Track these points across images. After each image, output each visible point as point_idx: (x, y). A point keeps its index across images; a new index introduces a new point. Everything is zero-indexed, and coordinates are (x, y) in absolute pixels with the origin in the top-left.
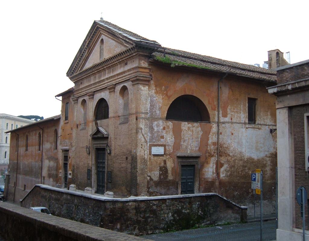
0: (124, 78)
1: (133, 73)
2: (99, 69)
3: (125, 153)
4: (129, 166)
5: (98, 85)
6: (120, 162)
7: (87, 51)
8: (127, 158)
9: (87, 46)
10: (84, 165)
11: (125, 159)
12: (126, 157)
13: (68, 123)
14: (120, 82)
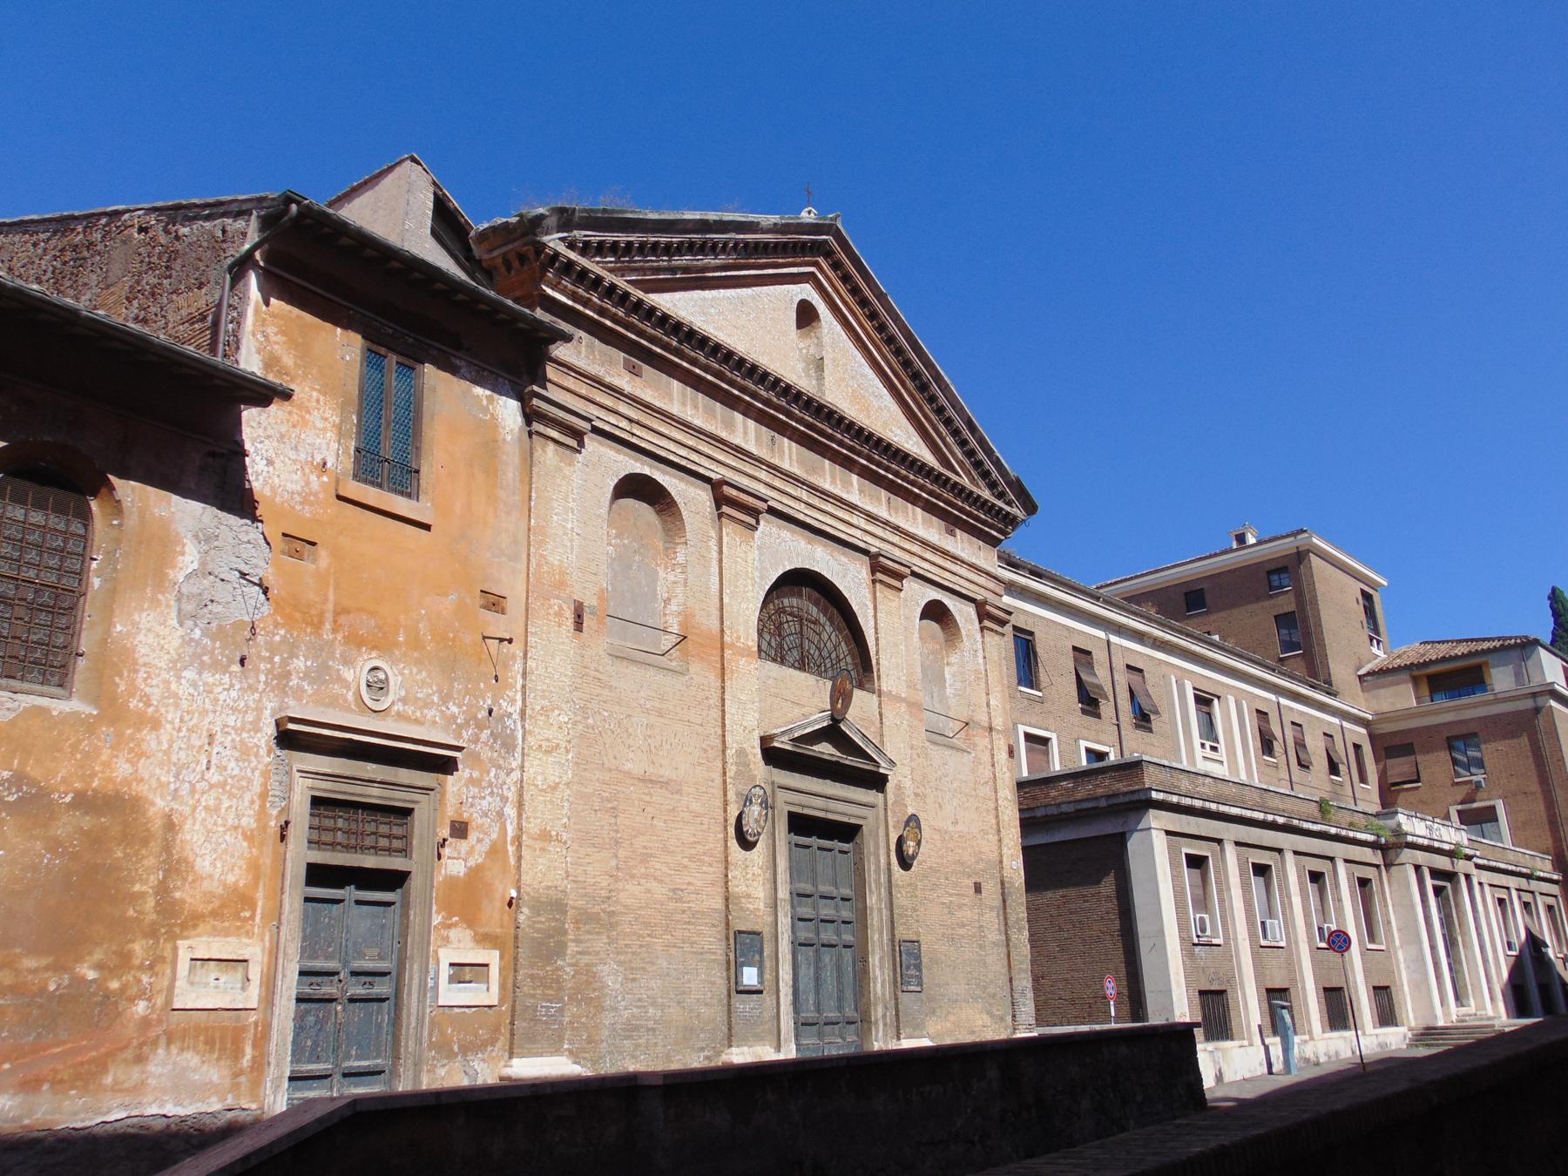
0: (947, 575)
2: (830, 438)
3: (968, 867)
6: (951, 902)
8: (978, 888)
10: (680, 900)
12: (975, 883)
13: (427, 527)
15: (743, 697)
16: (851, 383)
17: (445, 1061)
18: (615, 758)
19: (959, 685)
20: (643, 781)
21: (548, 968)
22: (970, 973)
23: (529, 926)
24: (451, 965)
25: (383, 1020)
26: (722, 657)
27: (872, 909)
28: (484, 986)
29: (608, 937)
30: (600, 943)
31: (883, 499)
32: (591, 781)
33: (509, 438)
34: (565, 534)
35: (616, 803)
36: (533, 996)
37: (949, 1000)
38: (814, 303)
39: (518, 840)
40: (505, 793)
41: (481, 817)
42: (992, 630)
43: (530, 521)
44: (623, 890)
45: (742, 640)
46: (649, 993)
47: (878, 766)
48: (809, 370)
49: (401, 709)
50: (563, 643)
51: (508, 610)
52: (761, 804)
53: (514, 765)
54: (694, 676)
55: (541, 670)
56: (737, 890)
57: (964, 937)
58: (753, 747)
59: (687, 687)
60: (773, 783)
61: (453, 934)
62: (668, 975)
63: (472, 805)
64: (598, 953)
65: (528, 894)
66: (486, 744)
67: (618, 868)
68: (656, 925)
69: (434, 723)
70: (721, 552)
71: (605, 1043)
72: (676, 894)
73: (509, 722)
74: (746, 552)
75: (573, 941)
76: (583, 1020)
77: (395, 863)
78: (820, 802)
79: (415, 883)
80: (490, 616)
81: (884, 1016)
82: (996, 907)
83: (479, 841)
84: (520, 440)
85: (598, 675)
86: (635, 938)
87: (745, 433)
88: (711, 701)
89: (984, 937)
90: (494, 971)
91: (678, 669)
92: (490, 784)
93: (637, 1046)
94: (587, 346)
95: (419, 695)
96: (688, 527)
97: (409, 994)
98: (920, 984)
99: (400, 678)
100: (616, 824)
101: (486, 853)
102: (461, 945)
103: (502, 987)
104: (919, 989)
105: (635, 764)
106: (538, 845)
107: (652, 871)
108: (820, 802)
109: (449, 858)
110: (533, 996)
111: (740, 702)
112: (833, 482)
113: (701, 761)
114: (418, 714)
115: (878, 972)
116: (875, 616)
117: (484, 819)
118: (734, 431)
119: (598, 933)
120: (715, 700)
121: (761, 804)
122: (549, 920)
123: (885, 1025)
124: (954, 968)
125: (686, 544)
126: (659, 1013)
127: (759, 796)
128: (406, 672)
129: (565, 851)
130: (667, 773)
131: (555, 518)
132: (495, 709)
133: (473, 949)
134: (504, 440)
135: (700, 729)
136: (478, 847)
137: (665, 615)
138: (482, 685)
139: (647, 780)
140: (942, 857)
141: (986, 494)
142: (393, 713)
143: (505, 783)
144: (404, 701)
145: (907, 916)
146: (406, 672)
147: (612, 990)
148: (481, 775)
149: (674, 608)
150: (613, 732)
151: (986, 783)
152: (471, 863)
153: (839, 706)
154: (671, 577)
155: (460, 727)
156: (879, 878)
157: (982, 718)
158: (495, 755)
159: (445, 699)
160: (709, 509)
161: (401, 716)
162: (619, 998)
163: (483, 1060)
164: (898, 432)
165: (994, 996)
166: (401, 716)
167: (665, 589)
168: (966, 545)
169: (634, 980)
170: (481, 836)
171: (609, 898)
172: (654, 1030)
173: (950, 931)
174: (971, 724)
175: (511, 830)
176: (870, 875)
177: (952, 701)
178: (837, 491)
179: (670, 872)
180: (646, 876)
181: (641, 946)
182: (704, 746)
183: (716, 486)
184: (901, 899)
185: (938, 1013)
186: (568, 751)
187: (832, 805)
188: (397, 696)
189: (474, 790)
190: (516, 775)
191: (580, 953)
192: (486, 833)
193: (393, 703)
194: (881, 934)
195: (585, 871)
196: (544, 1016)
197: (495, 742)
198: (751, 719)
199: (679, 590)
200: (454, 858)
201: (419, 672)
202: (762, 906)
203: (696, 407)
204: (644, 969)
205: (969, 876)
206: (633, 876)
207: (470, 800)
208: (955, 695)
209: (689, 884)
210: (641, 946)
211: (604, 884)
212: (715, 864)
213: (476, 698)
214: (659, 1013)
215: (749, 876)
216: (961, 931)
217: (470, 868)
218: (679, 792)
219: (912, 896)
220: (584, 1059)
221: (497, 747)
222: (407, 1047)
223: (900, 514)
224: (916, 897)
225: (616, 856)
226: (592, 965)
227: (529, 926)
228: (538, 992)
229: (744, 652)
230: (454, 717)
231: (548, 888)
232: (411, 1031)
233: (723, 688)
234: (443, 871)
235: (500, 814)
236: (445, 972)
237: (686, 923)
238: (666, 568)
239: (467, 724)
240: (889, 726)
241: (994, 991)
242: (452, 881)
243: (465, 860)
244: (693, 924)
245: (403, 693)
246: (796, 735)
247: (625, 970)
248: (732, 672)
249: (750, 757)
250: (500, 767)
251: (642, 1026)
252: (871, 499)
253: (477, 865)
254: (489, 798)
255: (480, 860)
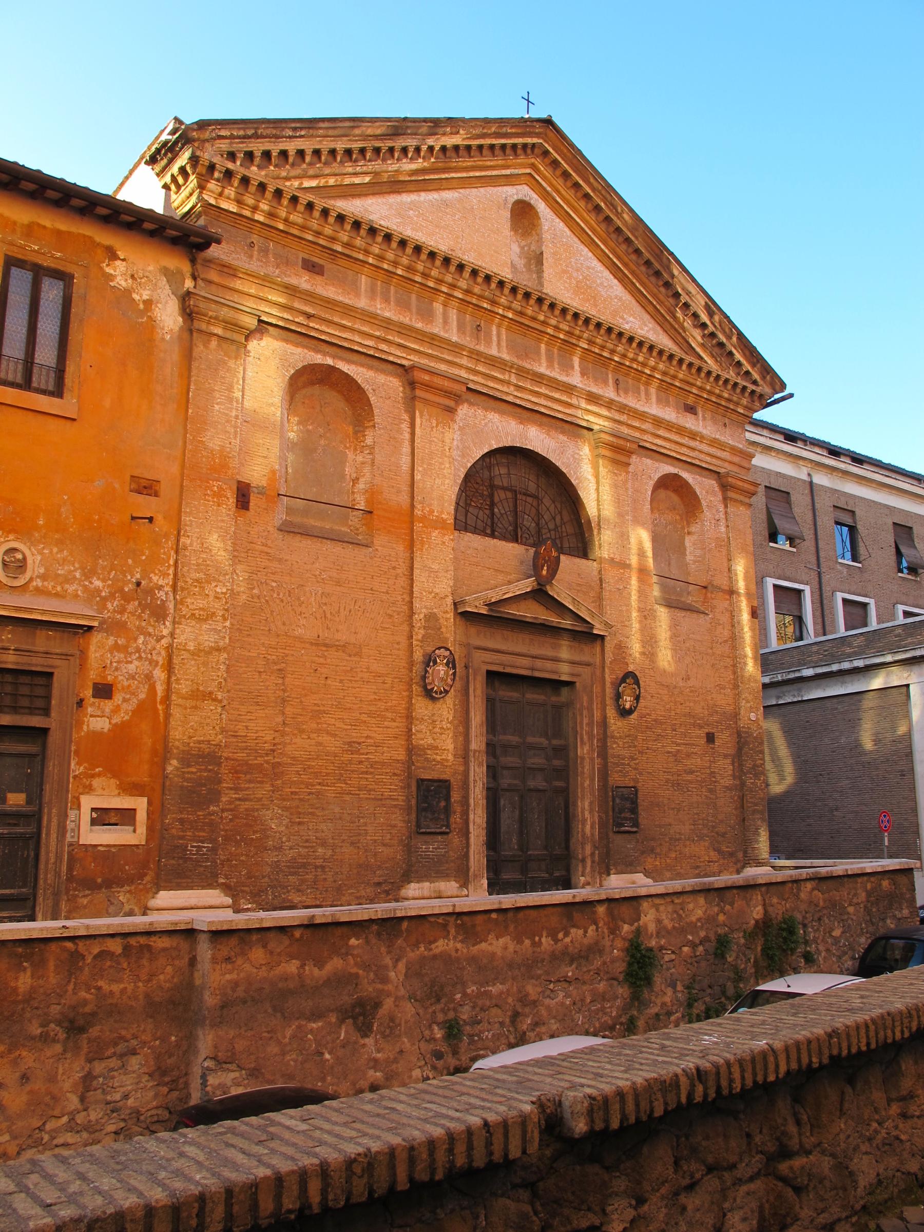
0: (684, 450)
1: (730, 462)
4: (725, 767)
5: (543, 390)
6: (678, 750)
7: (419, 164)
8: (710, 738)
9: (444, 149)
10: (358, 752)
11: (703, 741)
12: (708, 734)
13: (74, 420)
14: (663, 451)
15: (435, 566)
16: (575, 274)
17: (87, 892)
18: (284, 624)
19: (698, 552)
20: (317, 645)
21: (200, 813)
22: (697, 814)
23: (178, 776)
24: (93, 809)
25: (28, 855)
26: (412, 530)
27: (583, 758)
28: (131, 828)
29: (272, 785)
30: (263, 791)
31: (611, 381)
32: (255, 645)
33: (168, 337)
34: (228, 421)
35: (284, 665)
36: (182, 838)
37: (671, 839)
38: (532, 202)
39: (167, 698)
40: (155, 658)
41: (127, 679)
42: (736, 501)
43: (187, 411)
44: (290, 744)
45: (436, 514)
46: (318, 835)
47: (592, 626)
48: (530, 265)
49: (40, 584)
50: (223, 521)
51: (162, 493)
52: (447, 664)
53: (165, 632)
54: (379, 548)
55: (196, 546)
56: (422, 742)
57: (691, 782)
58: (446, 612)
59: (371, 558)
60: (468, 644)
61: (96, 782)
62: (340, 818)
63: (117, 669)
64: (260, 799)
65: (178, 748)
66: (133, 614)
67: (284, 723)
68: (327, 774)
69: (77, 596)
70: (413, 434)
71: (266, 879)
72: (352, 746)
73: (161, 594)
74: (443, 433)
75: (231, 789)
76: (243, 858)
77: (36, 721)
78: (525, 662)
79: (54, 738)
80: (141, 499)
81: (592, 854)
82: (730, 755)
83: (125, 700)
84: (180, 338)
85: (266, 549)
86: (303, 786)
87: (446, 322)
88: (399, 571)
89: (715, 782)
90: (141, 816)
91: (364, 542)
92: (138, 650)
93: (303, 881)
94: (260, 250)
95: (59, 572)
96: (376, 411)
97: (48, 834)
98: (636, 824)
99: (39, 557)
100: (283, 684)
101: (133, 712)
102: (105, 793)
103: (150, 829)
104: (634, 829)
105: (305, 629)
106: (189, 703)
107: (325, 726)
108: (526, 662)
109: (92, 716)
110: (182, 838)
111: (431, 570)
112: (550, 365)
113: (384, 625)
114: (59, 588)
115: (587, 814)
116: (597, 489)
117: (131, 681)
118: (431, 322)
119: (261, 782)
120: (402, 569)
121: (447, 664)
122: (200, 770)
123: (593, 862)
124: (679, 810)
125: (374, 427)
126: (330, 852)
127: (445, 657)
128: (46, 551)
129: (219, 710)
130: (343, 636)
131: (217, 407)
132: (143, 582)
133: (119, 794)
134: (163, 339)
135: (384, 597)
136: (125, 706)
137: (353, 493)
138: (130, 561)
139: (317, 643)
140: (670, 710)
141: (731, 374)
142: (31, 588)
143: (154, 649)
144: (44, 577)
145: (623, 764)
146: (46, 551)
147: (276, 832)
148: (128, 642)
149: (361, 486)
150: (282, 601)
151: (726, 641)
152: (116, 720)
153: (544, 572)
154: (360, 458)
155: (104, 599)
156: (592, 730)
157: (721, 581)
158: (144, 624)
159: (89, 574)
160: (401, 395)
161: (39, 591)
162: (284, 839)
163: (130, 892)
164: (631, 319)
165: (723, 835)
166: (39, 591)
167: (354, 469)
168: (709, 423)
169: (300, 823)
170: (128, 696)
171: (273, 751)
172: (323, 867)
173: (675, 777)
174: (710, 587)
175: (160, 689)
176: (582, 728)
177: (693, 567)
178: (556, 374)
179: (346, 727)
180: (318, 731)
181: (310, 794)
182: (389, 612)
183: (405, 372)
184: (616, 748)
185: (658, 850)
186: (225, 619)
187: (539, 664)
188: (36, 573)
189: (119, 656)
190: (164, 642)
191: (239, 799)
192: (134, 694)
193: (31, 579)
194: (592, 780)
195: (247, 727)
196: (194, 854)
197: (143, 612)
198: (444, 586)
199: (367, 470)
200: (98, 716)
201: (61, 551)
202: (450, 757)
203: (387, 300)
204: (313, 814)
205: (701, 727)
206: (302, 731)
207: (115, 664)
208: (695, 562)
209: (367, 737)
210: (310, 794)
211: (268, 738)
212: (399, 720)
213: (124, 573)
214: (330, 852)
215: (437, 730)
216: (689, 777)
217: (116, 725)
218: (358, 654)
219: (630, 747)
220: (243, 891)
221: (146, 617)
222: (46, 880)
223: (630, 393)
224: (635, 746)
225: (283, 714)
226: (253, 810)
227: (178, 776)
228: (188, 834)
229: (440, 524)
230: (98, 591)
231: (199, 742)
232: (50, 866)
233: (412, 558)
234: (85, 727)
235: (149, 677)
236: (86, 816)
237: (362, 773)
238: (355, 450)
239: (112, 596)
240: (610, 591)
241: (724, 830)
242: (96, 736)
243: (110, 718)
244: (371, 773)
245: (42, 571)
246: (493, 600)
247: (291, 814)
248: (422, 543)
249: (441, 621)
250: (150, 635)
251: (309, 864)
252: (596, 381)
253: (123, 723)
254: (136, 663)
255: (127, 718)
